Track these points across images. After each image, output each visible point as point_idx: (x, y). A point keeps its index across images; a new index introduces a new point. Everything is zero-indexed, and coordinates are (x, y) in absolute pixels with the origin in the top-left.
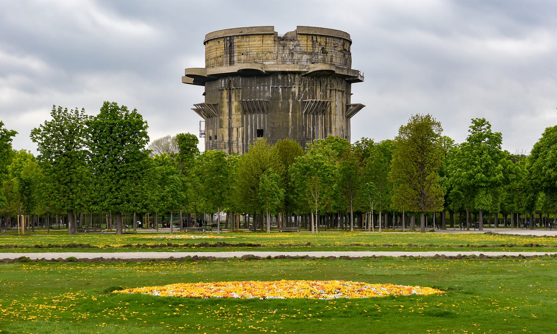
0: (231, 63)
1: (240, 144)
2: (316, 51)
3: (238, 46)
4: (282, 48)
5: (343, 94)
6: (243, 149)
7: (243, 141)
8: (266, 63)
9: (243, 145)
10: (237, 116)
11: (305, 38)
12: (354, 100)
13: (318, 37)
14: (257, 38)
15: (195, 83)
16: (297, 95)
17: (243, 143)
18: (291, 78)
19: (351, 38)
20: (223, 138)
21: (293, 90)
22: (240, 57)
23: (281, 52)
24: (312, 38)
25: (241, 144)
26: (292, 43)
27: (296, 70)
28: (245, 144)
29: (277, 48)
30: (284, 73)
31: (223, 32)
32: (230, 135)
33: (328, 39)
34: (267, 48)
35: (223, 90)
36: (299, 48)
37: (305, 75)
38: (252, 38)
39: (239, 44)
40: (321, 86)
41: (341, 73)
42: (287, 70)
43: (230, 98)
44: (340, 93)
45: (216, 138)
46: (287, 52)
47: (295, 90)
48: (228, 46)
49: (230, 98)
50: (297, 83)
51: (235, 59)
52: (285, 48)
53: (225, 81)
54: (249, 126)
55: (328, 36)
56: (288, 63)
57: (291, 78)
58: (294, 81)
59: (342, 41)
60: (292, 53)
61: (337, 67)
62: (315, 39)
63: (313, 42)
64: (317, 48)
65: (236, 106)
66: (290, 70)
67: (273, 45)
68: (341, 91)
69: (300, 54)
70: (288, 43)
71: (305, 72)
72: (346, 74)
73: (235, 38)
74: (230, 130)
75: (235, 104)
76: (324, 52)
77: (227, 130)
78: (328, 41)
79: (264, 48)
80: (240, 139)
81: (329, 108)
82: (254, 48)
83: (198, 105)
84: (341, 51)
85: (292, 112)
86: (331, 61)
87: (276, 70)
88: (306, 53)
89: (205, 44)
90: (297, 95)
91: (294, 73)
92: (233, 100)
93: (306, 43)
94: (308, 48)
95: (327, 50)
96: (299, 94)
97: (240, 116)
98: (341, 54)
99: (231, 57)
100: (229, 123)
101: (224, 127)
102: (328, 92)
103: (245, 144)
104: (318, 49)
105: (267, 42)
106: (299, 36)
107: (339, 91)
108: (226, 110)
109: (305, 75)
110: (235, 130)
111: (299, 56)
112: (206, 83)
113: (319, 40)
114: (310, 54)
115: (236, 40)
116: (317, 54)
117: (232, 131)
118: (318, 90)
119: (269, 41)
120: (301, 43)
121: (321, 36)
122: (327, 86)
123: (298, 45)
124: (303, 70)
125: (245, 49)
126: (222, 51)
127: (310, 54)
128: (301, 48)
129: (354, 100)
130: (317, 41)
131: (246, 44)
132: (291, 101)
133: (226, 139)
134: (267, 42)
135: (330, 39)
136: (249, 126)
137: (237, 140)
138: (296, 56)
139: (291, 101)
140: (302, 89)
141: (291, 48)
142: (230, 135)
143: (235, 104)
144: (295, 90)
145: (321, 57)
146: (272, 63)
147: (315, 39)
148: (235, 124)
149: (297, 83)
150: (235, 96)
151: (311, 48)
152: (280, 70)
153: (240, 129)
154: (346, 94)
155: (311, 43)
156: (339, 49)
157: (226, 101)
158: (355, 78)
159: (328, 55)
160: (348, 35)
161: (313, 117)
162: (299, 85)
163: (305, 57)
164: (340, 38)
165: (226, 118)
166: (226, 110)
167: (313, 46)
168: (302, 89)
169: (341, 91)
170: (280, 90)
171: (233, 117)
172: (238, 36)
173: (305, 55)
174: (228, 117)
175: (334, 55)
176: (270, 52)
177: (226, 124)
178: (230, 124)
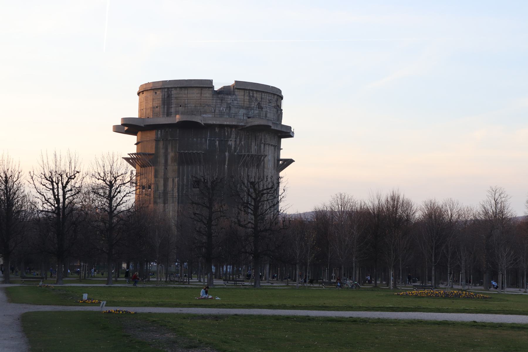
0: (169, 114)
1: (176, 194)
2: (252, 106)
3: (176, 98)
4: (220, 101)
5: (275, 149)
6: (178, 199)
7: (178, 190)
8: (204, 115)
9: (178, 195)
10: (172, 167)
11: (242, 92)
12: (284, 155)
13: (254, 92)
14: (196, 91)
15: (127, 132)
16: (233, 148)
17: (178, 193)
18: (228, 132)
19: (283, 94)
21: (230, 143)
22: (177, 108)
23: (219, 106)
24: (249, 93)
25: (177, 194)
26: (230, 97)
27: (234, 123)
28: (180, 194)
29: (215, 101)
30: (222, 126)
31: (161, 84)
32: (165, 185)
33: (263, 94)
34: (205, 101)
35: (159, 140)
36: (236, 102)
37: (241, 130)
38: (190, 91)
39: (178, 96)
40: (255, 140)
41: (275, 128)
42: (225, 123)
43: (166, 149)
44: (273, 147)
45: (150, 187)
46: (225, 105)
47: (232, 143)
48: (166, 97)
49: (166, 149)
50: (233, 136)
51: (173, 110)
52: (223, 101)
53: (161, 132)
54: (185, 177)
55: (263, 92)
56: (225, 116)
57: (228, 132)
58: (231, 135)
59: (276, 97)
60: (230, 107)
61: (273, 123)
62: (251, 94)
63: (250, 96)
64: (253, 103)
66: (228, 123)
67: (211, 98)
68: (274, 146)
69: (237, 108)
70: (226, 96)
71: (242, 126)
72: (280, 129)
73: (173, 89)
75: (171, 155)
76: (260, 107)
77: (162, 180)
78: (263, 96)
79: (202, 101)
80: (176, 190)
81: (262, 163)
82: (192, 101)
83: (132, 154)
84: (274, 107)
85: (227, 166)
86: (266, 116)
87: (215, 123)
88: (242, 107)
89: (139, 94)
90: (233, 148)
91: (231, 127)
92: (169, 150)
93: (243, 97)
94: (245, 103)
95: (262, 105)
96: (235, 148)
97: (177, 167)
98: (275, 110)
99: (169, 108)
102: (262, 146)
103: (180, 194)
104: (254, 105)
105: (205, 95)
106: (236, 90)
107: (272, 145)
108: (162, 160)
109: (241, 130)
110: (170, 180)
111: (236, 110)
112: (139, 133)
113: (255, 95)
114: (247, 108)
115: (174, 92)
116: (252, 109)
118: (253, 144)
119: (207, 94)
120: (238, 97)
121: (257, 91)
122: (261, 141)
123: (236, 100)
124: (241, 124)
125: (183, 101)
126: (159, 102)
127: (247, 108)
128: (239, 102)
129: (284, 155)
130: (253, 96)
131: (184, 96)
132: (227, 154)
133: (161, 188)
134: (205, 95)
135: (266, 94)
136: (185, 177)
137: (173, 190)
138: (233, 111)
139: (227, 154)
140: (238, 143)
141: (229, 102)
142: (165, 185)
143: (171, 155)
144: (232, 143)
145: (257, 112)
146: (210, 116)
147: (251, 94)
148: (170, 175)
149: (233, 136)
151: (248, 103)
152: (218, 123)
153: (176, 180)
154: (278, 149)
155: (247, 98)
156: (273, 105)
157: (162, 151)
158: (287, 133)
159: (263, 110)
160: (280, 91)
161: (248, 170)
162: (236, 138)
163: (242, 111)
164: (274, 94)
165: (161, 168)
166: (162, 160)
167: (250, 101)
168: (238, 143)
169: (274, 146)
170: (217, 142)
171: (168, 168)
172: (176, 88)
173: (242, 110)
174: (163, 167)
175: (269, 111)
176: (209, 106)
178: (165, 174)
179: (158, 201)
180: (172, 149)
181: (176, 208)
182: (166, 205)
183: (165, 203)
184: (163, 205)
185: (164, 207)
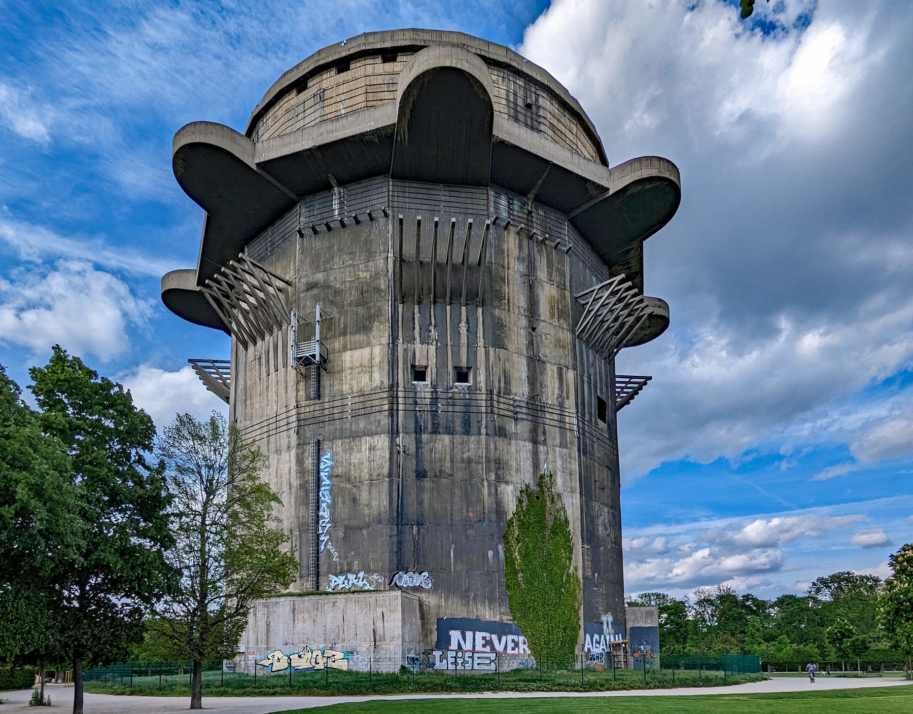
20: (507, 382)
32: (534, 380)
45: (462, 376)
65: (552, 297)
74: (535, 363)
80: (570, 404)
100: (531, 343)
101: (511, 347)
117: (543, 372)
133: (521, 390)
137: (561, 405)
148: (547, 351)
150: (550, 265)
153: (570, 375)
171: (542, 327)
174: (524, 322)
177: (518, 338)
179: (511, 427)
180: (550, 274)
181: (575, 466)
182: (541, 448)
183: (535, 442)
184: (529, 446)
185: (535, 454)
